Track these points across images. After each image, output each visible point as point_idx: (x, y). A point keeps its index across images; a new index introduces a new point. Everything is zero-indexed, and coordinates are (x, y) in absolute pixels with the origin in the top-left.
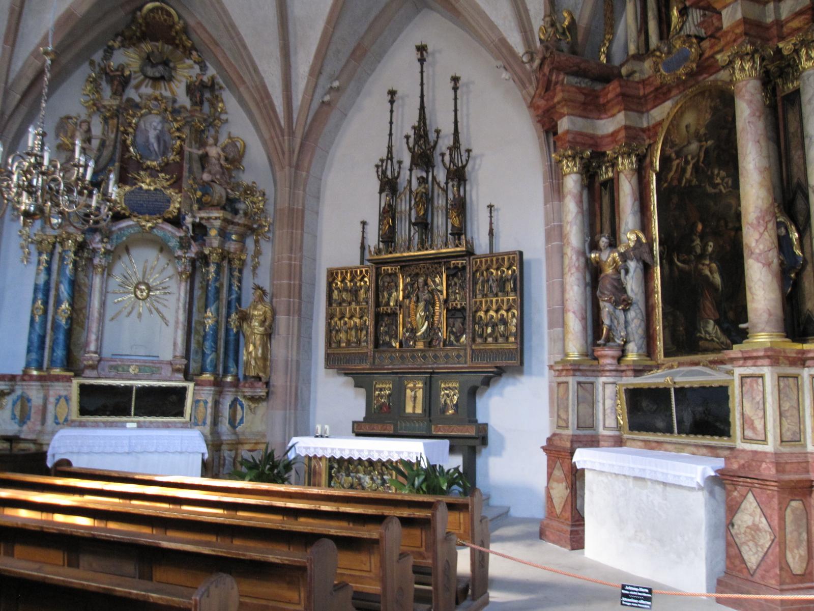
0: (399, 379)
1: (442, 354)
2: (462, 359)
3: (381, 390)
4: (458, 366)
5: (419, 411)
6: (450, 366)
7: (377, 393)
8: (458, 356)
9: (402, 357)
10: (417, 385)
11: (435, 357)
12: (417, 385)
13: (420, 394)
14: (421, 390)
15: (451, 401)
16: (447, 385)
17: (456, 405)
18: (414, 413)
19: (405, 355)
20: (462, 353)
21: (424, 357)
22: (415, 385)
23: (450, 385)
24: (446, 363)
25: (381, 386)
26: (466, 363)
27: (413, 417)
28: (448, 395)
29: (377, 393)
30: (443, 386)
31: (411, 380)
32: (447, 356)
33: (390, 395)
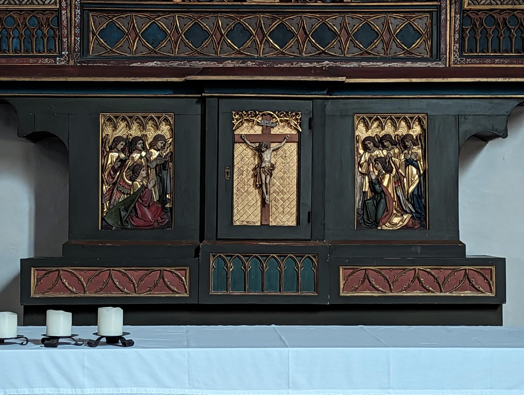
0: (207, 104)
1: (354, 23)
2: (420, 46)
3: (131, 145)
4: (409, 64)
5: (285, 214)
6: (380, 64)
7: (114, 155)
8: (409, 35)
9: (196, 34)
10: (274, 131)
11: (324, 34)
12: (274, 131)
13: (286, 160)
14: (291, 149)
15: (399, 180)
16: (374, 131)
17: (418, 199)
18: (265, 226)
19: (205, 25)
20: (421, 23)
21: (283, 35)
22: (266, 129)
23: (389, 129)
24: (365, 56)
25: (122, 131)
26: (436, 54)
27: (262, 239)
28: (386, 165)
29: (114, 155)
30: (361, 132)
31: (250, 113)
32: (368, 34)
33: (161, 167)
